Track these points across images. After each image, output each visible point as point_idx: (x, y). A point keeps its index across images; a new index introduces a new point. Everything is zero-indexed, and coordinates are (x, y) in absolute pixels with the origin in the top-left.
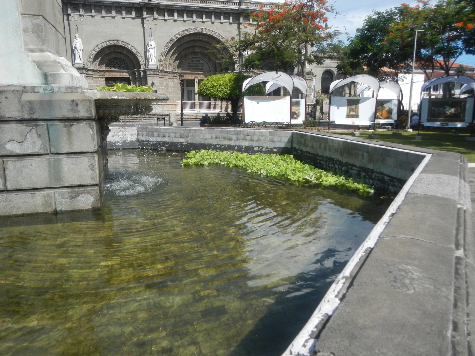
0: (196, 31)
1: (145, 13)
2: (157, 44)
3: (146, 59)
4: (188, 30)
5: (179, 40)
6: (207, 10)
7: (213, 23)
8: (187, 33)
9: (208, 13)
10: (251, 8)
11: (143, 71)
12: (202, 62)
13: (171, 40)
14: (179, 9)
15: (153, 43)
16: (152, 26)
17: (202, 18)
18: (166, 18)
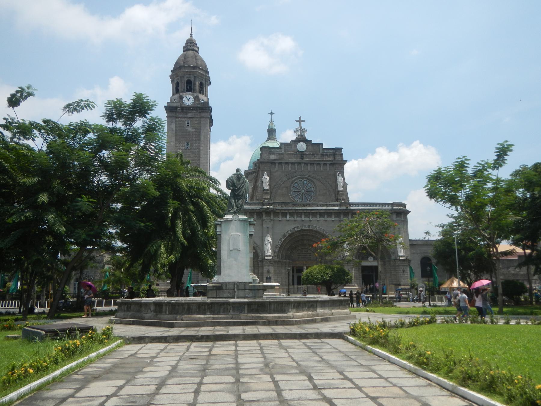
0: (304, 228)
1: (264, 216)
2: (273, 239)
3: (263, 252)
4: (297, 227)
5: (290, 235)
6: (313, 211)
7: (318, 221)
8: (296, 229)
9: (314, 213)
10: (349, 207)
11: (260, 261)
12: (309, 252)
13: (284, 236)
14: (291, 211)
15: (269, 239)
16: (270, 226)
17: (309, 217)
18: (280, 219)
